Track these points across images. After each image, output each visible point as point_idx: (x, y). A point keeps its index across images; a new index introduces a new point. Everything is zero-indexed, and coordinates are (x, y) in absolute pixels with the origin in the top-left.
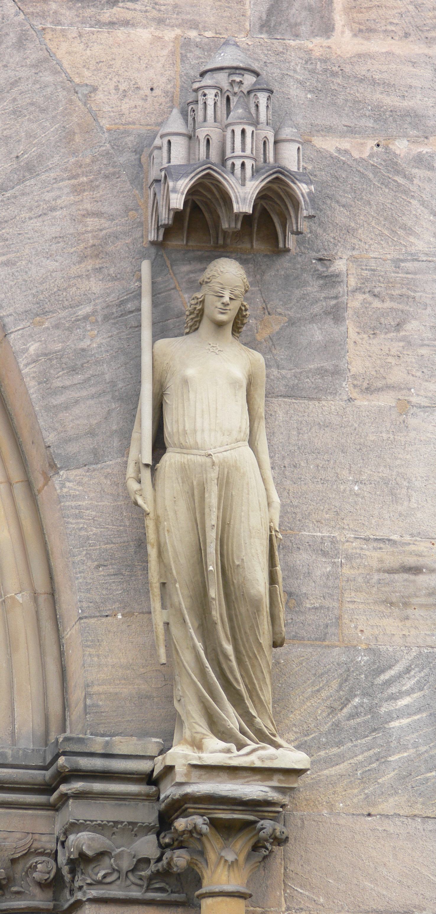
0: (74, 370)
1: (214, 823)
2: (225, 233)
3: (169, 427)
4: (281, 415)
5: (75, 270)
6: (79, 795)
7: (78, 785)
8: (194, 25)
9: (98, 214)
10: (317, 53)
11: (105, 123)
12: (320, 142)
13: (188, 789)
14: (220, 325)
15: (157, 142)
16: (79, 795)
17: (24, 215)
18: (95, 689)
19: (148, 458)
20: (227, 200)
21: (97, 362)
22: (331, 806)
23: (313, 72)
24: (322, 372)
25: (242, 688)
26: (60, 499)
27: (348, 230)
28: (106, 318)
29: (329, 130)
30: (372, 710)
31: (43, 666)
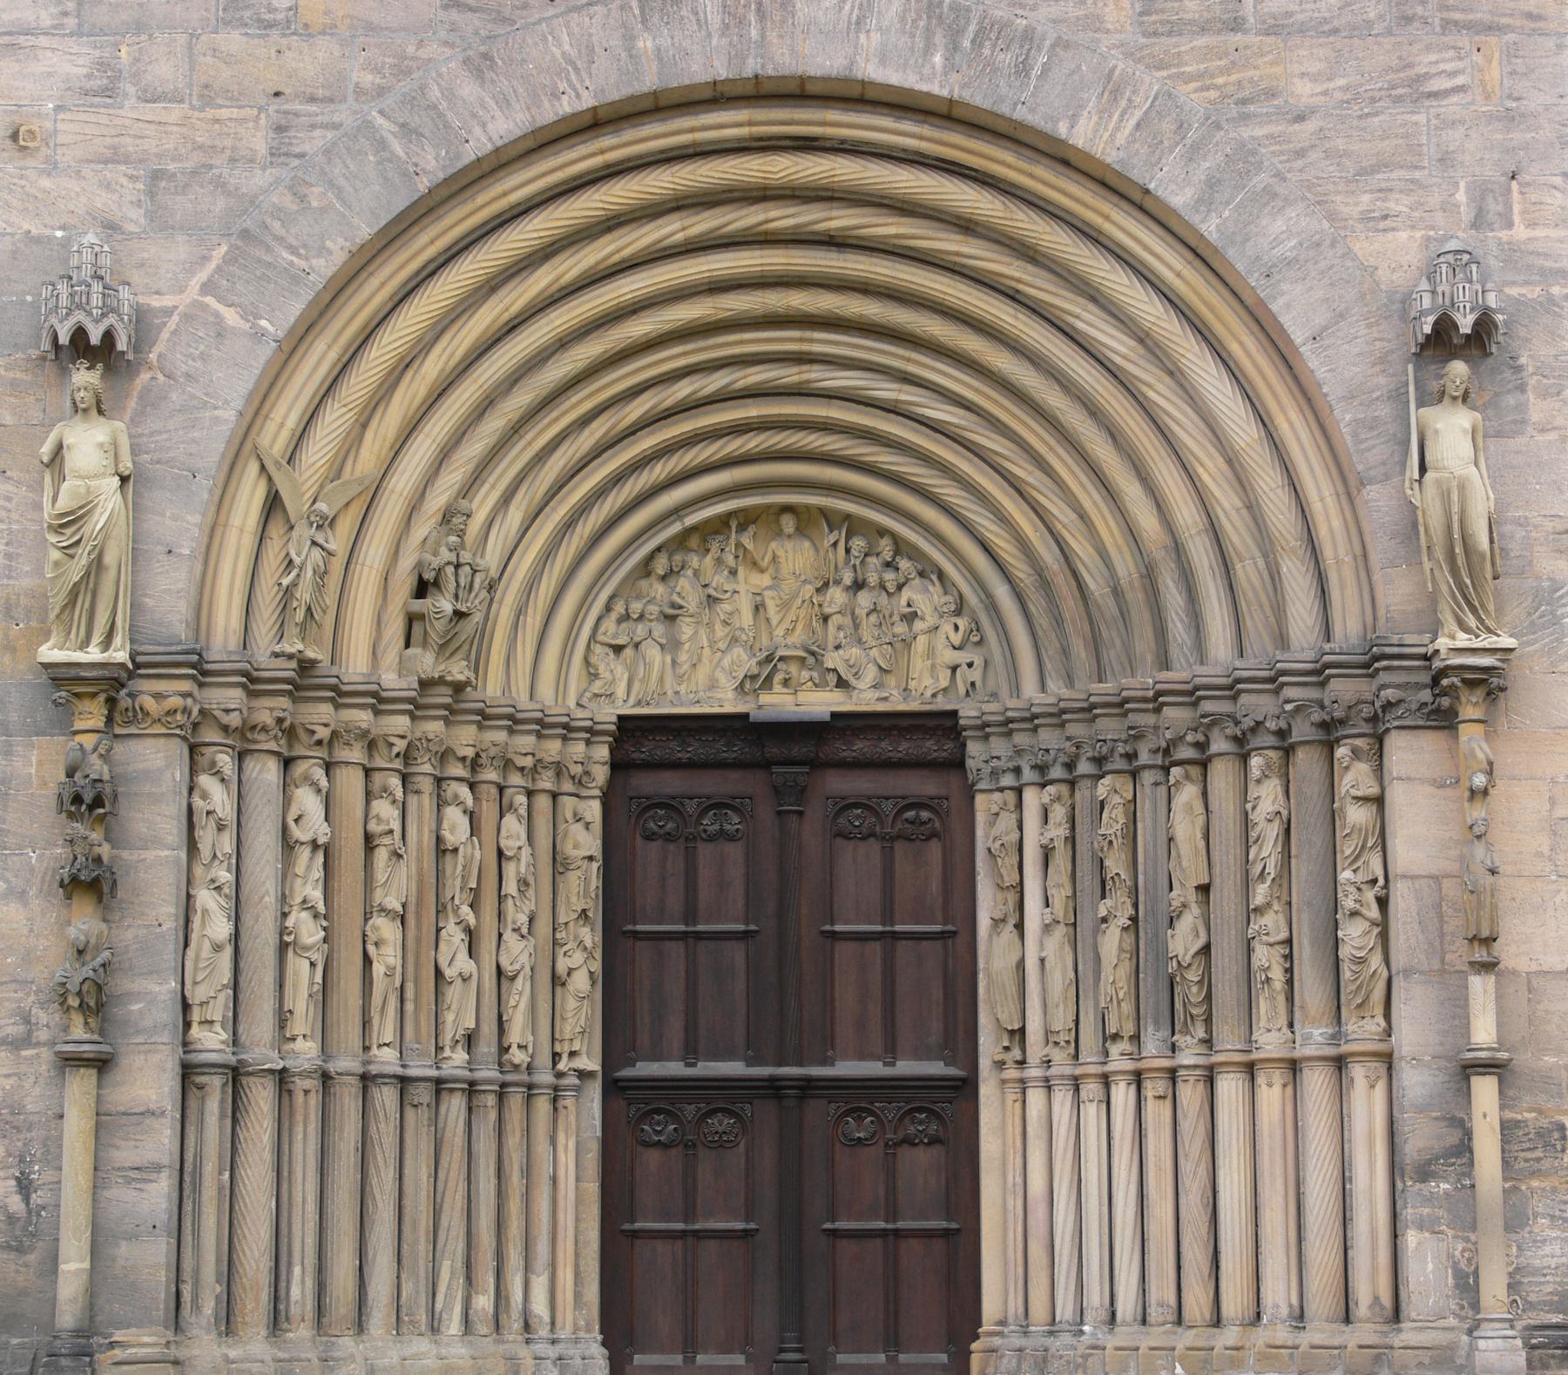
0: (1371, 428)
1: (1464, 681)
2: (1455, 346)
3: (1428, 458)
4: (1492, 448)
5: (1370, 372)
6: (1386, 668)
7: (1385, 663)
8: (1433, 228)
9: (1379, 340)
10: (1505, 239)
11: (1383, 287)
12: (1508, 290)
13: (1449, 662)
14: (1455, 398)
15: (1414, 296)
16: (1386, 668)
17: (1340, 342)
18: (1392, 608)
19: (1417, 476)
20: (1456, 327)
21: (1385, 423)
22: (1531, 669)
23: (1503, 250)
24: (1515, 422)
25: (1477, 604)
26: (1367, 502)
27: (1527, 340)
28: (1389, 398)
29: (1513, 283)
30: (1552, 613)
31: (1361, 597)
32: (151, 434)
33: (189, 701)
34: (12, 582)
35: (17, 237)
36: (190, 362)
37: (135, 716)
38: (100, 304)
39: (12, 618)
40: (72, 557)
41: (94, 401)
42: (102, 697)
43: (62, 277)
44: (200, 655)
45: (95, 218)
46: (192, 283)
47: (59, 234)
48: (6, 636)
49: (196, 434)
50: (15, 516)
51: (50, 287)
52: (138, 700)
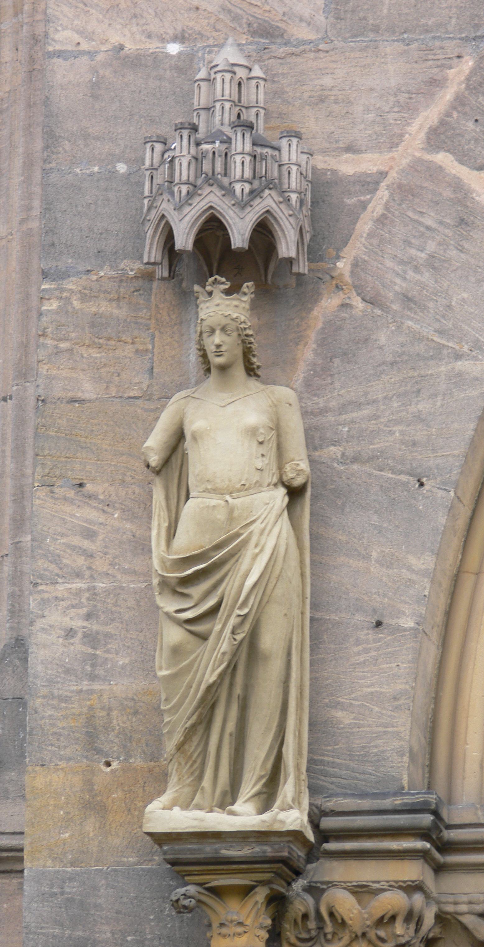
32: (343, 409)
33: (418, 899)
34: (97, 686)
35: (100, 57)
36: (411, 274)
37: (320, 928)
38: (248, 174)
39: (99, 751)
40: (204, 637)
41: (239, 352)
42: (261, 894)
43: (179, 128)
44: (435, 813)
45: (236, 18)
46: (413, 128)
47: (174, 49)
48: (89, 783)
49: (424, 406)
50: (100, 565)
51: (159, 147)
52: (326, 898)
